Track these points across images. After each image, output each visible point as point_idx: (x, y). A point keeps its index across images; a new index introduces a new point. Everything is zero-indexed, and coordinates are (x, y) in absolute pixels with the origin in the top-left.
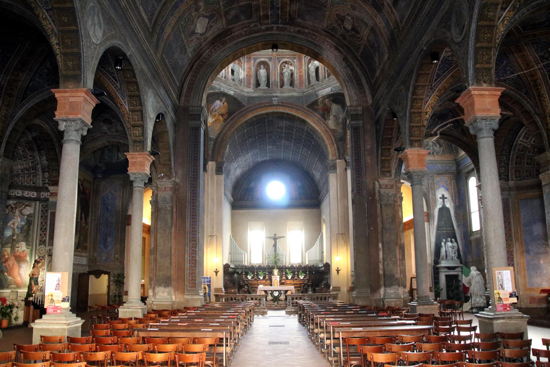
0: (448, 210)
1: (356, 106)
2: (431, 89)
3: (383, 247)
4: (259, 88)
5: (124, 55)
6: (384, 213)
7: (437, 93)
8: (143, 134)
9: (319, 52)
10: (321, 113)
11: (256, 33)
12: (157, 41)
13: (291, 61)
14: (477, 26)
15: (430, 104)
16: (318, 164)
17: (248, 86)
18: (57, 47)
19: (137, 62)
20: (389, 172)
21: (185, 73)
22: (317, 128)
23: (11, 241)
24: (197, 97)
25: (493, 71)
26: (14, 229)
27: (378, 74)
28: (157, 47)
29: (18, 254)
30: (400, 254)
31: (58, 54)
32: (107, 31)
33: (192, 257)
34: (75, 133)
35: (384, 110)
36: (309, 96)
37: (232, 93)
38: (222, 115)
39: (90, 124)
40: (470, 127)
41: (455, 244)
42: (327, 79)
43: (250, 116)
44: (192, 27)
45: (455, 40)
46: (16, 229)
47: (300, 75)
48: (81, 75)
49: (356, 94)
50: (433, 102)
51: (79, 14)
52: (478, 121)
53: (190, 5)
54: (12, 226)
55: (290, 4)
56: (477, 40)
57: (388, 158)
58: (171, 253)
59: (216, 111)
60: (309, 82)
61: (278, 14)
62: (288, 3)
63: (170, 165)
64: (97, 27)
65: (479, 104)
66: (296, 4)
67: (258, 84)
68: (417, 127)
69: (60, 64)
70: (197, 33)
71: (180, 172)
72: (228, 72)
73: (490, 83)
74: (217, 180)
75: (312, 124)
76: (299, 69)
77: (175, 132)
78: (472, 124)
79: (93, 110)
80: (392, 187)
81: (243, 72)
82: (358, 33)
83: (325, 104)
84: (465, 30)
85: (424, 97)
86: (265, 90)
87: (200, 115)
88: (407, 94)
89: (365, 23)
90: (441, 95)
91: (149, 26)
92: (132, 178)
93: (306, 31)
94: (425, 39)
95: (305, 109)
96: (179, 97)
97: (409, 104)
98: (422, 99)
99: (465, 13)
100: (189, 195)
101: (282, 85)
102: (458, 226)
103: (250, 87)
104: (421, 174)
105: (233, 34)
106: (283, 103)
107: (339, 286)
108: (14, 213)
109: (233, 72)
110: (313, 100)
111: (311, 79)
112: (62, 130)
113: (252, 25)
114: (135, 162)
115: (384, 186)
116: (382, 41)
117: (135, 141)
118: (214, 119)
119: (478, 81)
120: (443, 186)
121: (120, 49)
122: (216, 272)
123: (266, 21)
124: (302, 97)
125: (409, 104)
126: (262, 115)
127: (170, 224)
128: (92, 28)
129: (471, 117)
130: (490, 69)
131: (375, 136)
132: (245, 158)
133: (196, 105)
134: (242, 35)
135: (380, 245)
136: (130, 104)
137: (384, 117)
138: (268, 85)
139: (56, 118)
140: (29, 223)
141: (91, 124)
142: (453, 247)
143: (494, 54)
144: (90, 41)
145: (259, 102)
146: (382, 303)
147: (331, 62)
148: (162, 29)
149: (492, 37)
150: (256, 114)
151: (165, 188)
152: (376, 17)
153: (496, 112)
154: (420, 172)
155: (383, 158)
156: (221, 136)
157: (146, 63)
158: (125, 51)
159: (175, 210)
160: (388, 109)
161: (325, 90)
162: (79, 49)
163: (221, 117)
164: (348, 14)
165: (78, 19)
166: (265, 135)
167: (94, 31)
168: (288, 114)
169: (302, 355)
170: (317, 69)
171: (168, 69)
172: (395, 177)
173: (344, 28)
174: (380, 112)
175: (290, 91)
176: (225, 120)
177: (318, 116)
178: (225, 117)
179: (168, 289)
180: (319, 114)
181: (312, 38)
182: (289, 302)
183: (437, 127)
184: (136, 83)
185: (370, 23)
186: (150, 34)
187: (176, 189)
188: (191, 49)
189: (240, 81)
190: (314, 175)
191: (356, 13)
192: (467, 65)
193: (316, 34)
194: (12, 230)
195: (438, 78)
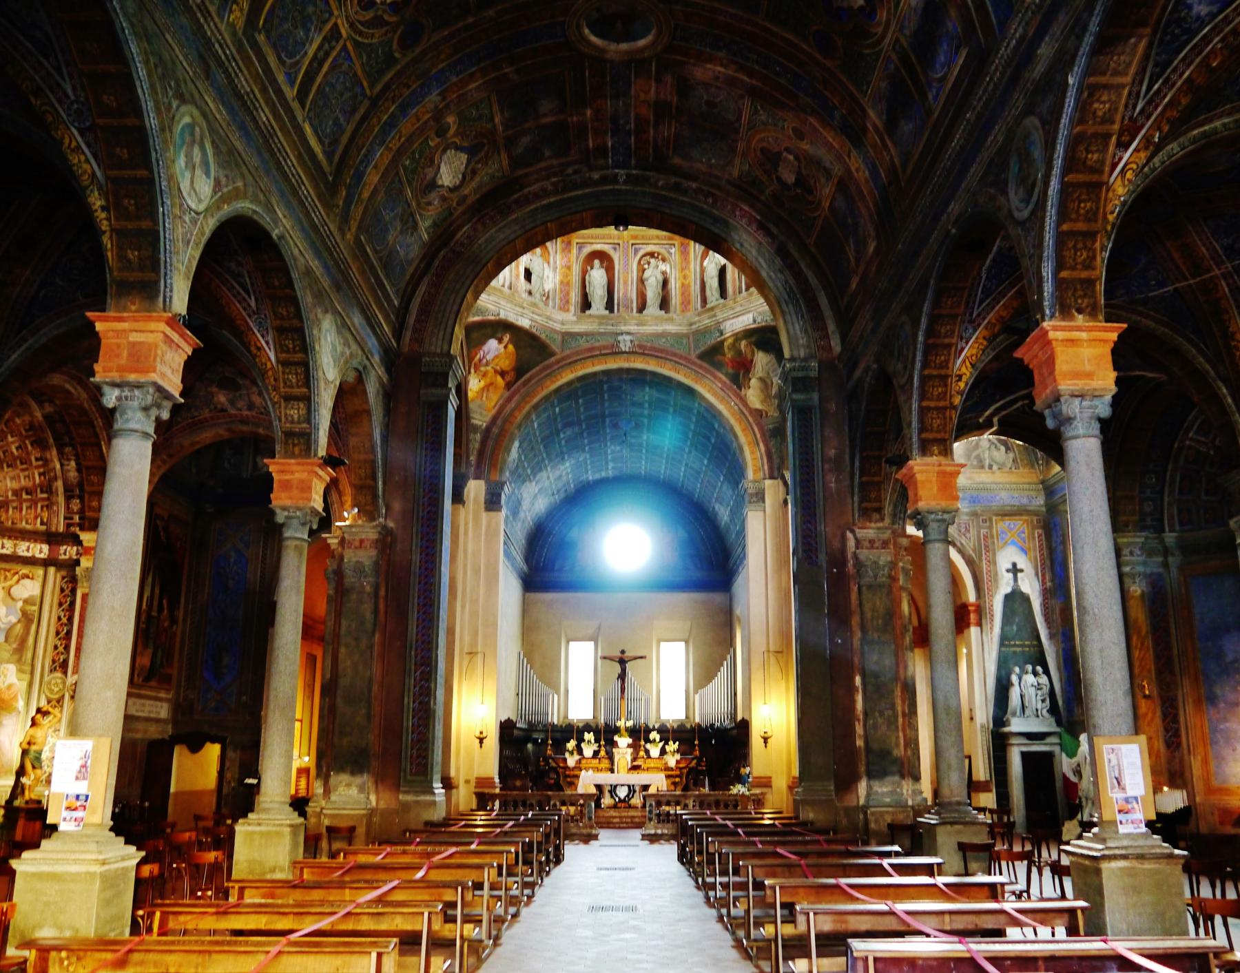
0: (1026, 599)
1: (805, 360)
2: (971, 322)
3: (864, 683)
4: (588, 312)
5: (266, 234)
6: (867, 607)
7: (986, 333)
8: (309, 417)
9: (723, 235)
10: (730, 371)
11: (576, 188)
12: (345, 202)
13: (663, 251)
14: (1062, 183)
15: (967, 359)
16: (725, 488)
17: (564, 307)
18: (103, 215)
19: (296, 252)
20: (879, 510)
21: (412, 276)
22: (721, 407)
24: (441, 333)
25: (1100, 288)
27: (854, 286)
28: (345, 219)
30: (903, 702)
31: (104, 232)
32: (223, 180)
33: (420, 703)
34: (139, 415)
35: (867, 369)
36: (705, 331)
37: (525, 323)
38: (503, 374)
39: (177, 395)
40: (1047, 412)
41: (1044, 679)
42: (744, 293)
43: (568, 376)
44: (430, 172)
45: (1016, 214)
47: (683, 285)
48: (158, 282)
49: (806, 331)
50: (974, 351)
51: (156, 142)
52: (1062, 400)
53: (426, 122)
56: (1063, 216)
57: (876, 479)
58: (370, 691)
59: (487, 364)
60: (704, 301)
63: (375, 488)
64: (198, 172)
65: (1064, 360)
67: (586, 304)
68: (937, 409)
69: (109, 254)
70: (442, 186)
71: (397, 506)
72: (518, 276)
73: (1093, 314)
74: (489, 525)
75: (708, 396)
76: (682, 270)
77: (388, 411)
78: (1049, 407)
79: (186, 363)
80: (885, 544)
81: (551, 275)
82: (811, 192)
83: (739, 352)
84: (1037, 190)
85: (954, 341)
86: (603, 317)
87: (445, 377)
88: (915, 336)
89: (825, 168)
90: (995, 336)
91: (327, 169)
92: (280, 518)
93: (694, 185)
94: (954, 208)
95: (694, 363)
96: (398, 333)
97: (919, 357)
98: (949, 346)
99: (1037, 153)
100: (416, 558)
101: (642, 307)
102: (1052, 636)
103: (568, 310)
104: (946, 516)
105: (526, 190)
106: (642, 350)
107: (768, 774)
109: (528, 274)
110: (711, 341)
111: (708, 293)
112: (111, 406)
113: (570, 171)
114: (288, 481)
115: (866, 544)
116: (863, 211)
117: (289, 434)
118: (482, 383)
119: (1065, 309)
120: (1013, 543)
121: (255, 223)
122: (481, 740)
123: (602, 162)
124: (686, 336)
125: (919, 357)
126: (595, 374)
127: (369, 626)
128: (188, 175)
129: (1048, 391)
130: (1091, 283)
131: (846, 428)
132: (557, 473)
133: (439, 351)
134: (544, 193)
135: (858, 680)
136: (280, 348)
137: (866, 385)
138: (610, 306)
139: (97, 379)
141: (181, 395)
142: (1039, 687)
143: (1103, 248)
144: (181, 205)
145: (588, 345)
146: (861, 816)
147: (749, 257)
148: (359, 177)
149: (1098, 208)
150: (581, 373)
151: (362, 541)
152: (849, 157)
153: (1106, 380)
154: (944, 512)
155: (864, 479)
156: (499, 422)
157: (318, 254)
158: (267, 227)
159: (382, 593)
160: (875, 366)
161: (741, 318)
162: (156, 223)
163: (499, 378)
164: (788, 150)
165: (154, 155)
166: (604, 422)
167: (192, 182)
168: (654, 374)
169: (662, 937)
170: (722, 272)
171: (372, 267)
172: (893, 523)
173: (778, 178)
174: (857, 374)
175: (658, 320)
176: (508, 386)
177: (724, 378)
178: (508, 378)
179: (358, 780)
180: (726, 375)
181: (706, 203)
182: (650, 812)
183: (993, 408)
184: (294, 301)
185: (837, 169)
186: (328, 188)
187: (386, 542)
188: (428, 223)
189: (546, 296)
190: (716, 514)
192: (1039, 272)
193: (717, 192)
195: (987, 298)
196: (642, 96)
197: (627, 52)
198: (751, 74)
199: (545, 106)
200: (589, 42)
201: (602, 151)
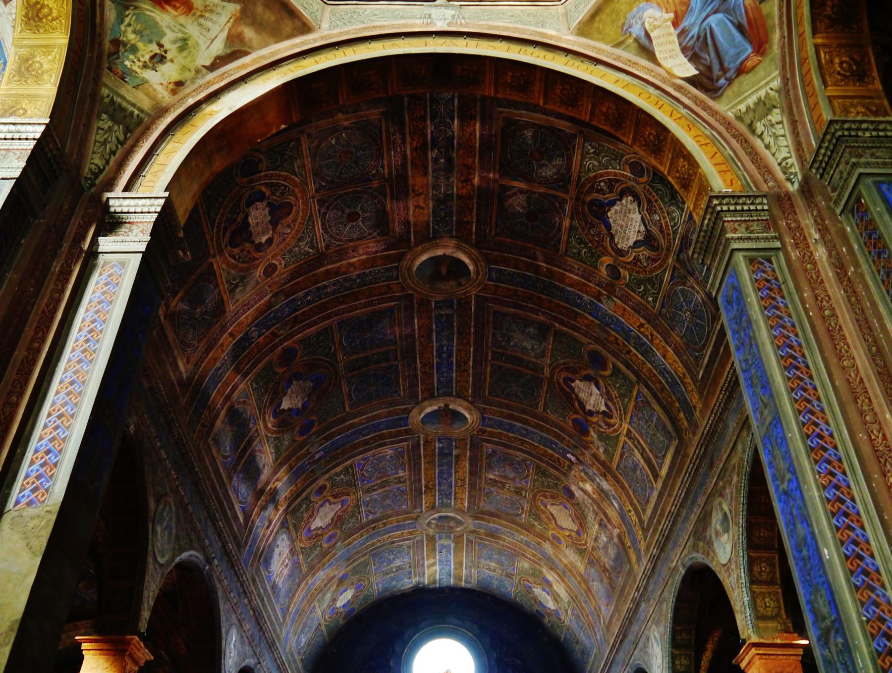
55: (404, 165)
61: (432, 120)
62: (409, 165)
66: (390, 173)
164: (270, 241)
173: (261, 197)
191: (259, 272)
196: (422, 198)
197: (437, 246)
198: (328, 274)
199: (518, 203)
200: (471, 258)
201: (466, 117)
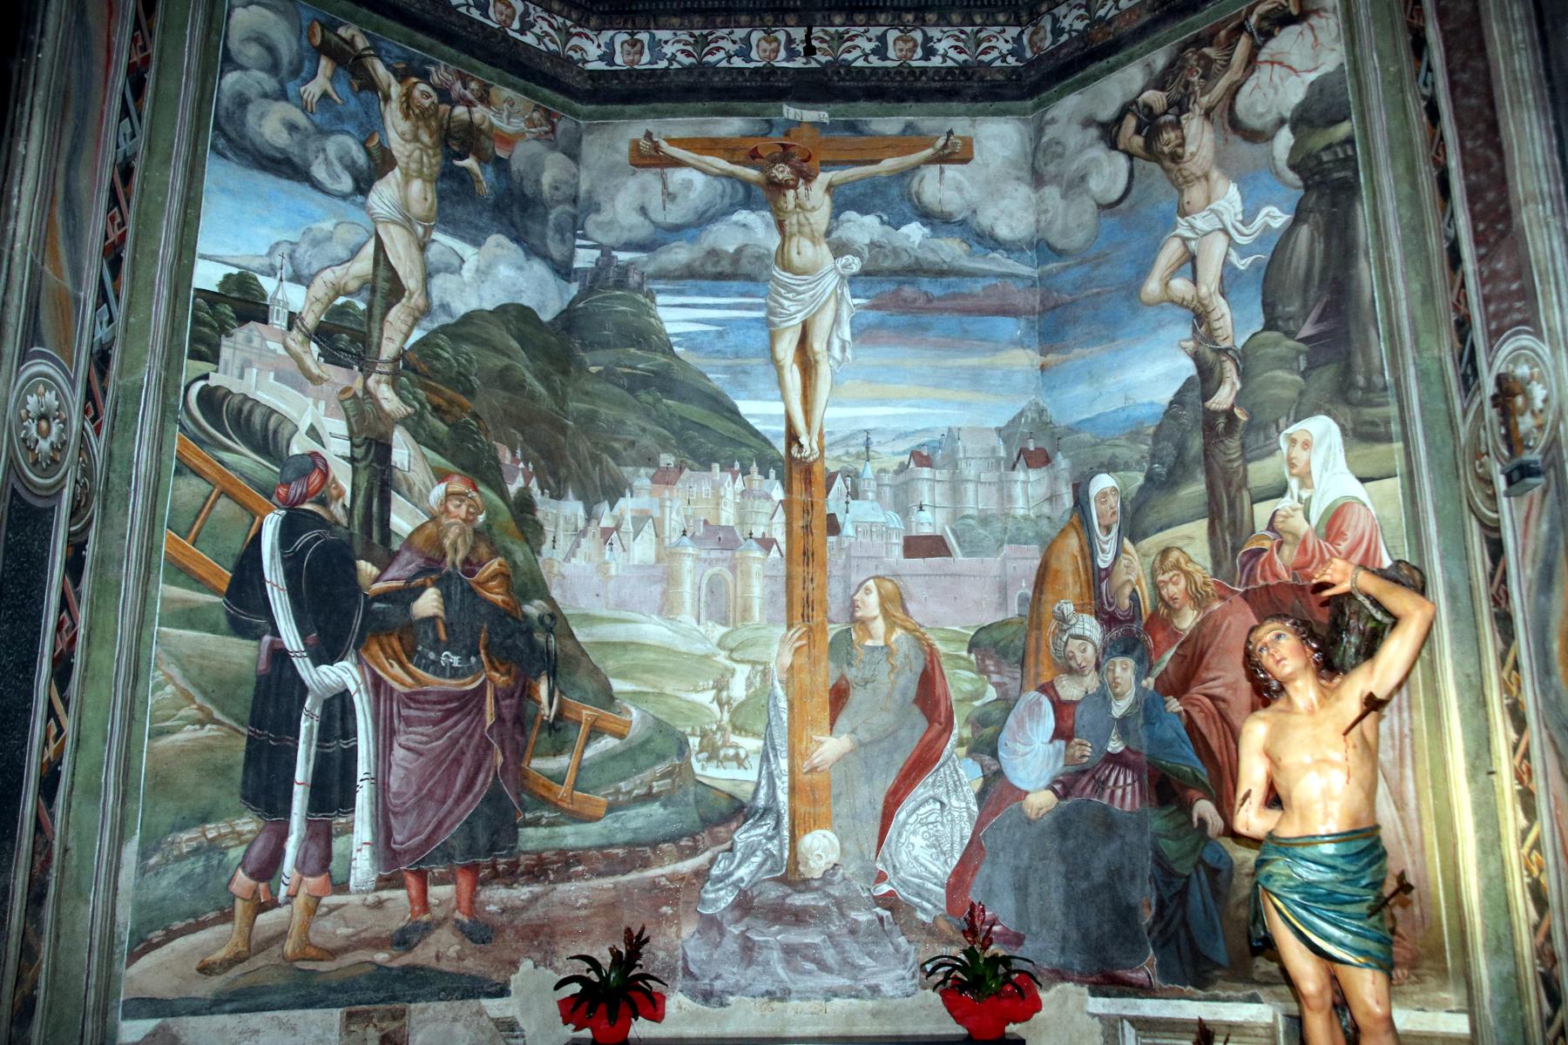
23: (1196, 444)
26: (1200, 316)
29: (1284, 562)
46: (1221, 307)
54: (1180, 286)
108: (1176, 158)
140: (1328, 187)
194: (1182, 331)
